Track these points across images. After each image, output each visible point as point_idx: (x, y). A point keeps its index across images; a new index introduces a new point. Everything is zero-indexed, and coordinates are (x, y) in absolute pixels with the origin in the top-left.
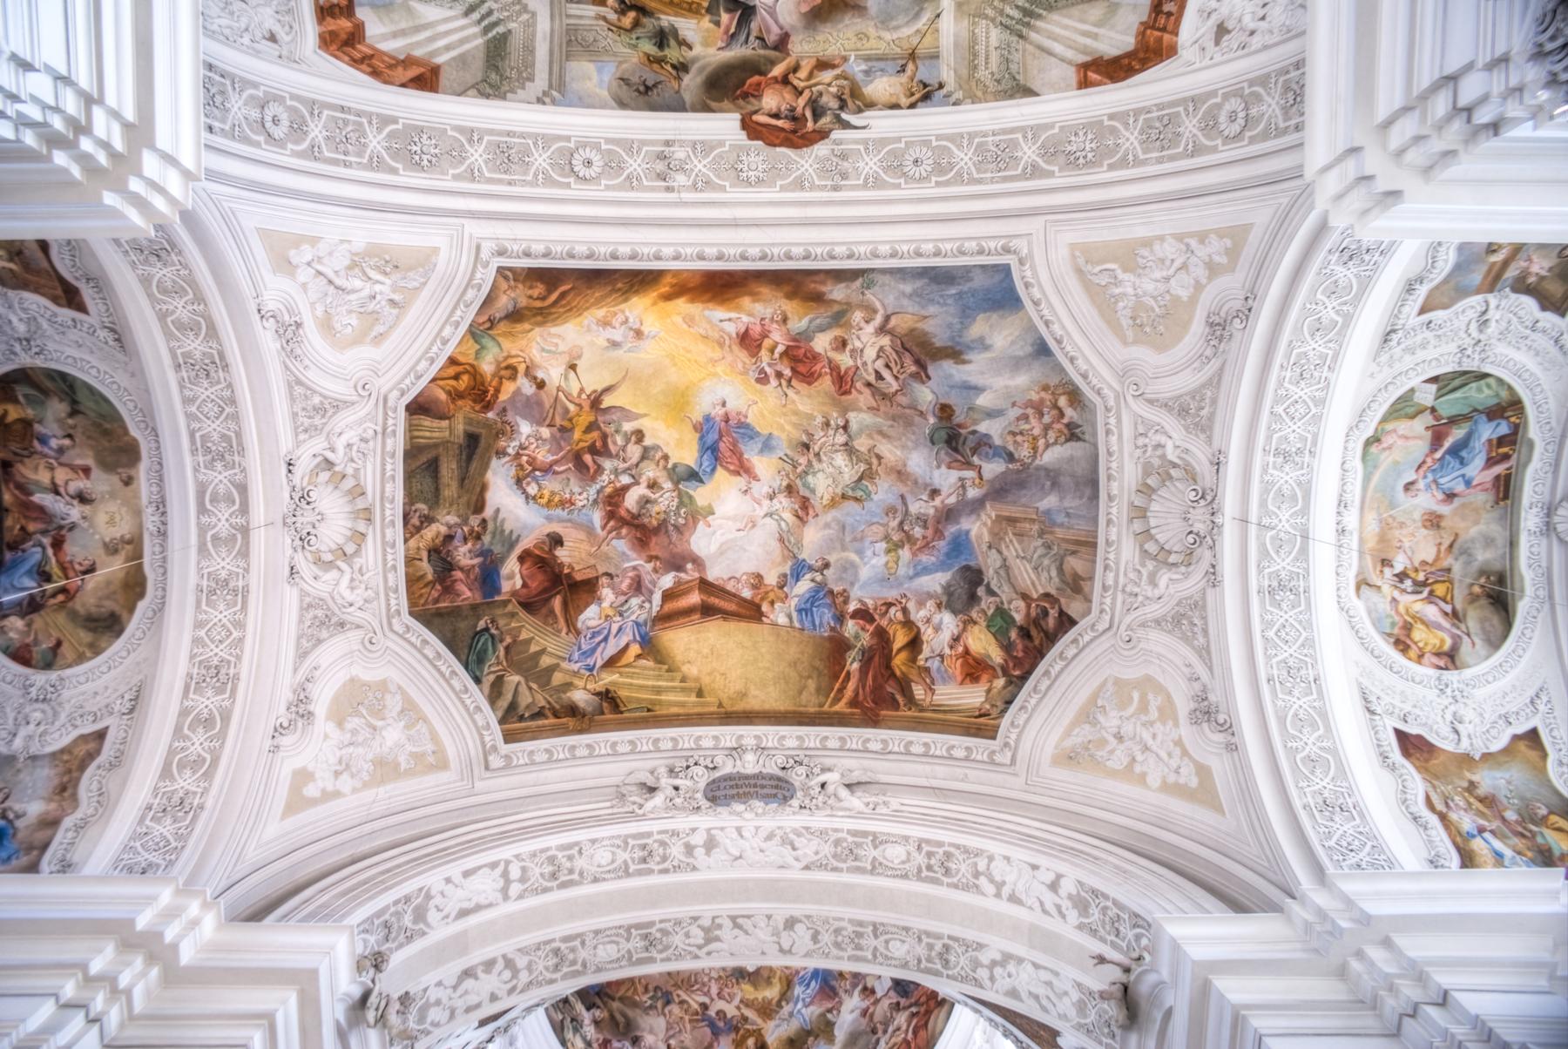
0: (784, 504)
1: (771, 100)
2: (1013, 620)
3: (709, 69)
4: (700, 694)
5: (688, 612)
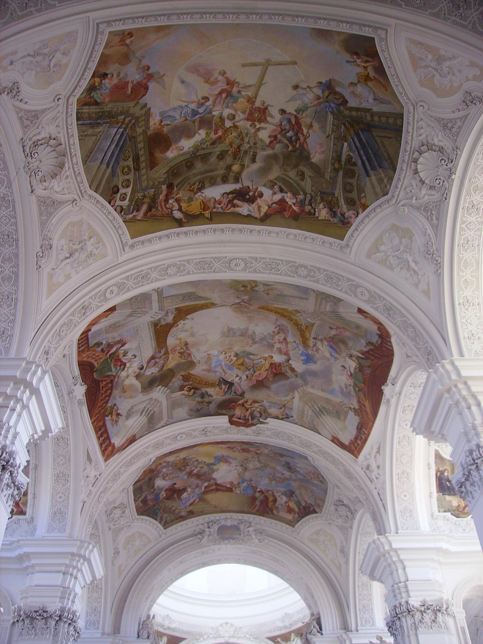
0: (240, 469)
1: (238, 412)
2: (302, 505)
3: (218, 402)
5: (212, 490)
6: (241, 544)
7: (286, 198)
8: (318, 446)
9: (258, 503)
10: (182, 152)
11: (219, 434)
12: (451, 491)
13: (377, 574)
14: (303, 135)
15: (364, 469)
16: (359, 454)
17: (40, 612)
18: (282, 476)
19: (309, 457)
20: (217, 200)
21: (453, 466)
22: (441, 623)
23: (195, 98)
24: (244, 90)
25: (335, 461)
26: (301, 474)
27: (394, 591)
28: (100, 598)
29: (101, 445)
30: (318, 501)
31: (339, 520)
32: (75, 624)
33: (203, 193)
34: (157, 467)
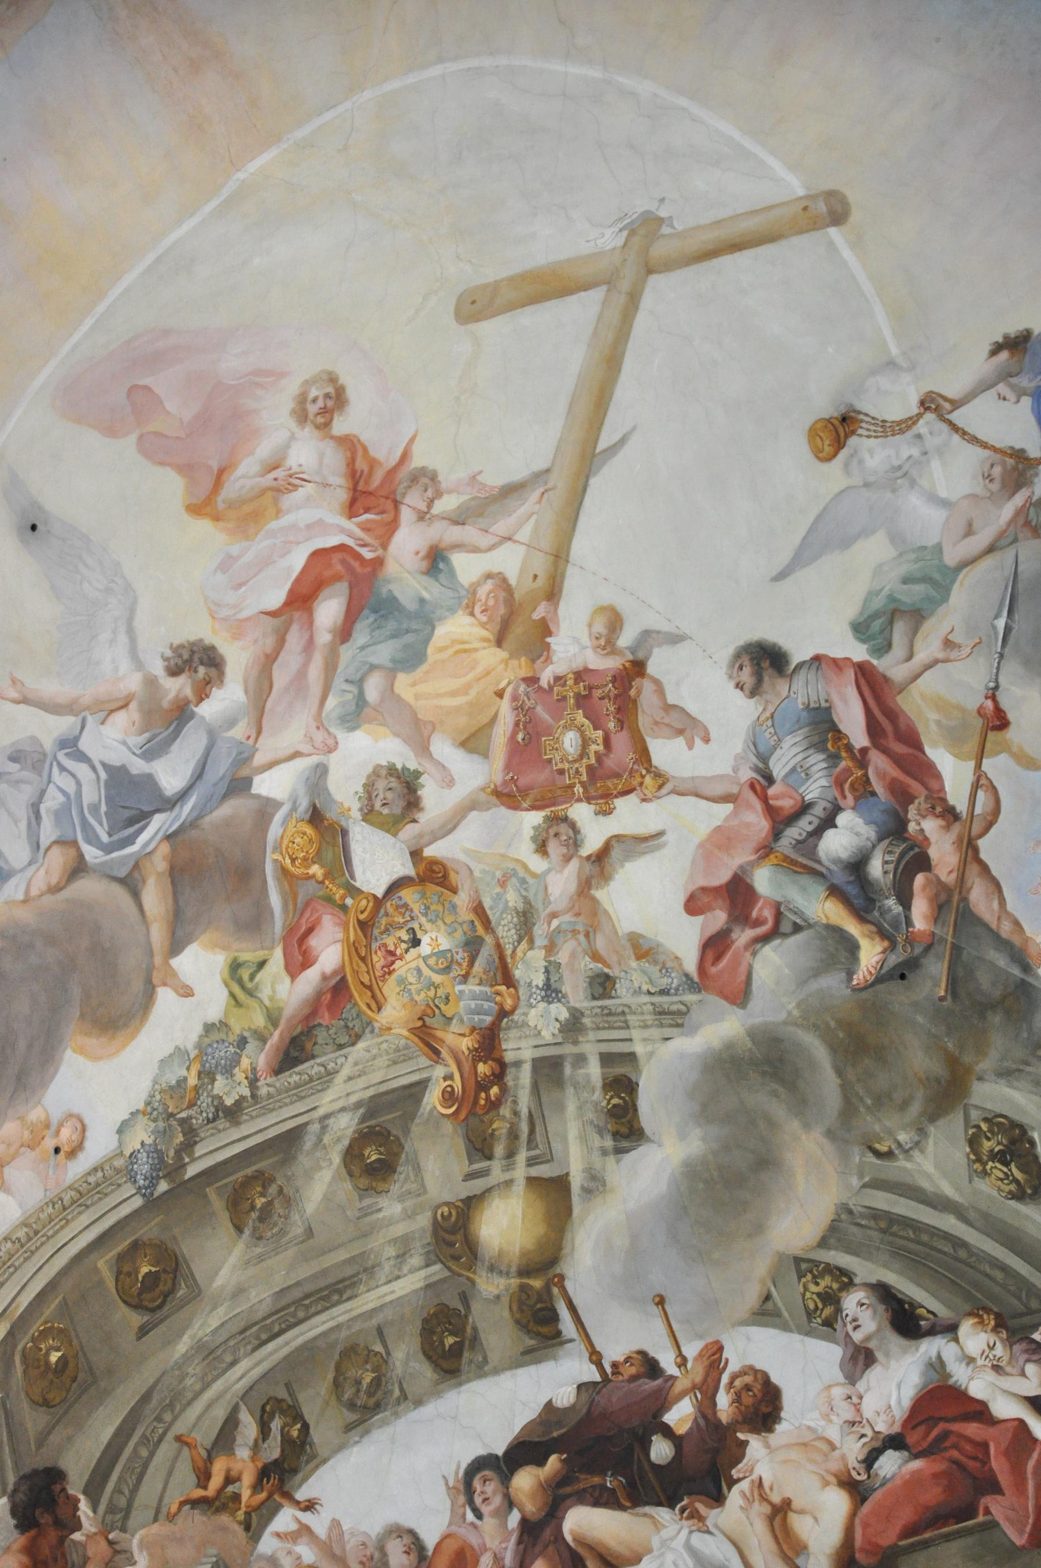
7: (959, 1374)
10: (77, 1168)
14: (950, 815)
20: (430, 1541)
23: (125, 666)
24: (469, 533)
33: (310, 1506)
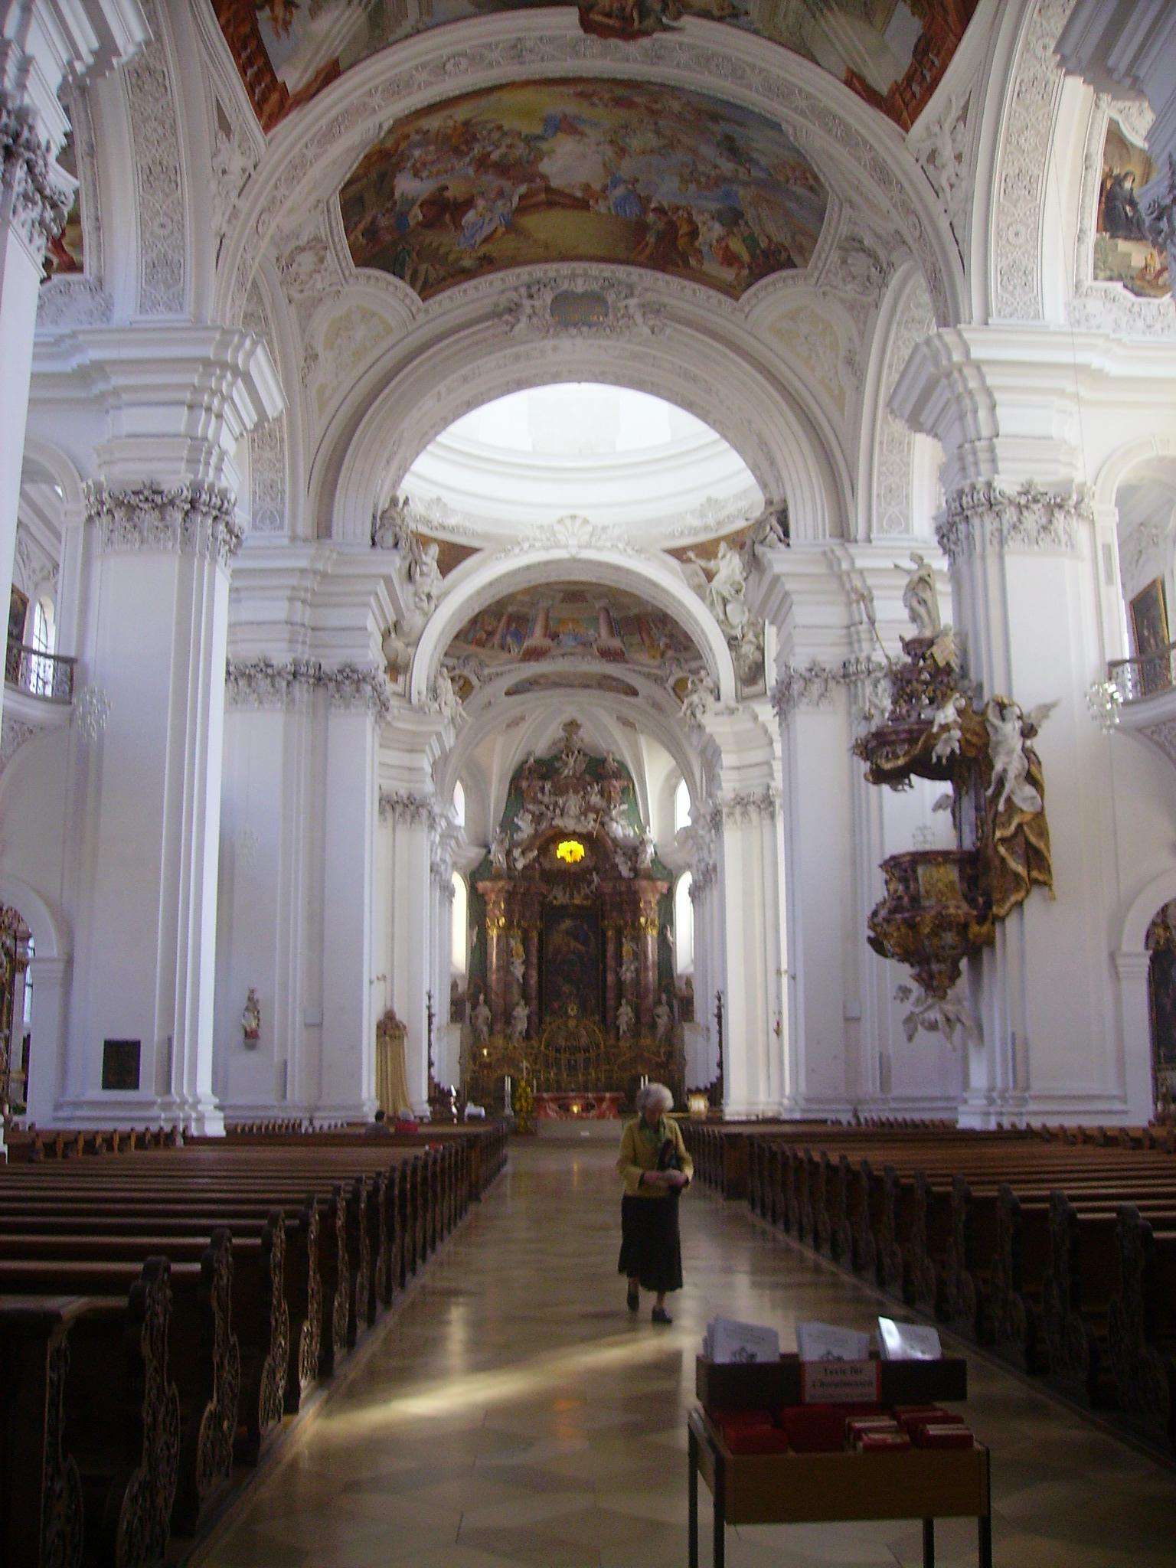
0: (609, 152)
4: (547, 247)
6: (608, 337)
8: (809, 96)
9: (651, 239)
11: (553, 58)
12: (1134, 229)
13: (927, 417)
15: (923, 161)
16: (912, 123)
17: (146, 493)
18: (713, 173)
19: (784, 126)
21: (1148, 164)
22: (1061, 532)
25: (850, 138)
26: (761, 169)
27: (961, 458)
28: (281, 460)
29: (251, 88)
30: (799, 238)
31: (849, 287)
32: (227, 518)
34: (397, 144)
